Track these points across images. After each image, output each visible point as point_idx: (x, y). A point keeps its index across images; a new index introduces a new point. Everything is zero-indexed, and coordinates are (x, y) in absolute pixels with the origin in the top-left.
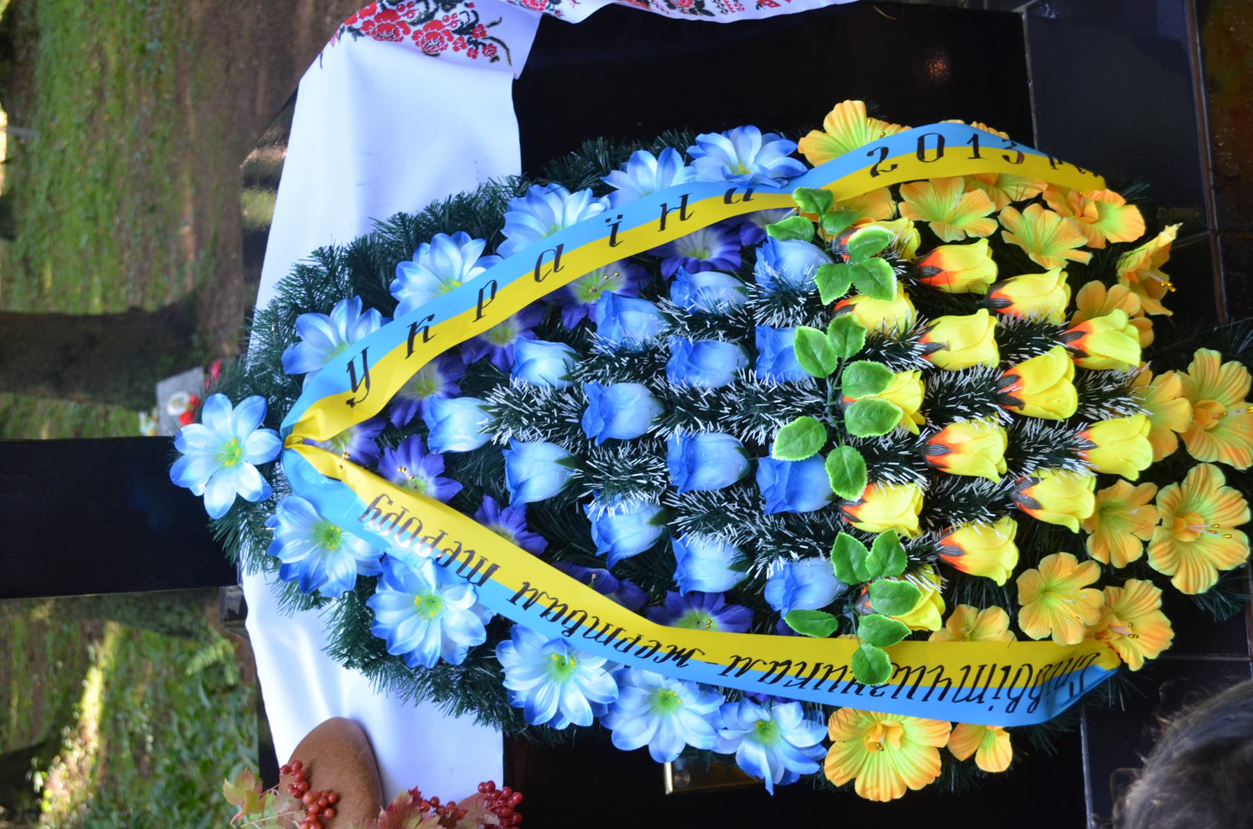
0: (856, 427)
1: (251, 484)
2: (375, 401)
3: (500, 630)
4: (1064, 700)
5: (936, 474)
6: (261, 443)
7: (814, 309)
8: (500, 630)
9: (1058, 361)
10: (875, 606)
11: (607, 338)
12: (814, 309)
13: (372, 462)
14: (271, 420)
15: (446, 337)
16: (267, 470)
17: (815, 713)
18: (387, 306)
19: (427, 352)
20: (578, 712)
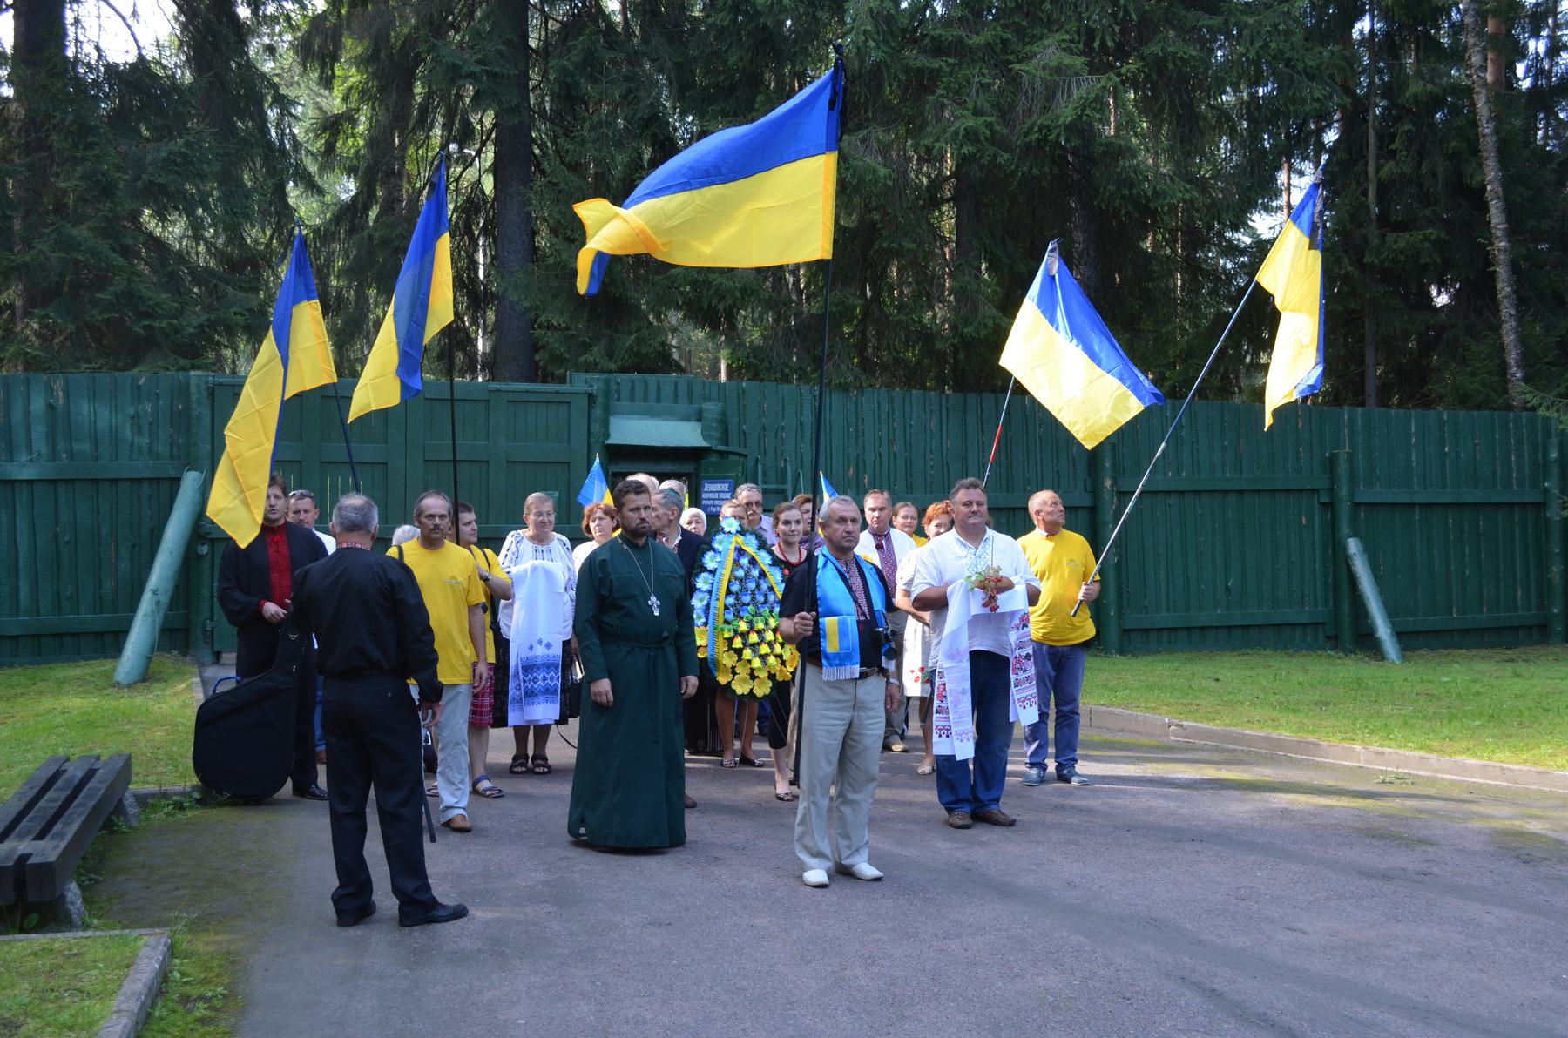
0: (755, 619)
1: (727, 530)
2: (744, 548)
3: (711, 572)
4: (711, 666)
5: (748, 633)
6: (733, 531)
7: (771, 612)
8: (713, 572)
9: (769, 651)
10: (727, 627)
11: (762, 581)
12: (771, 612)
13: (736, 549)
14: (737, 532)
15: (757, 558)
16: (730, 532)
17: (706, 624)
18: (759, 549)
19: (754, 555)
20: (698, 585)
